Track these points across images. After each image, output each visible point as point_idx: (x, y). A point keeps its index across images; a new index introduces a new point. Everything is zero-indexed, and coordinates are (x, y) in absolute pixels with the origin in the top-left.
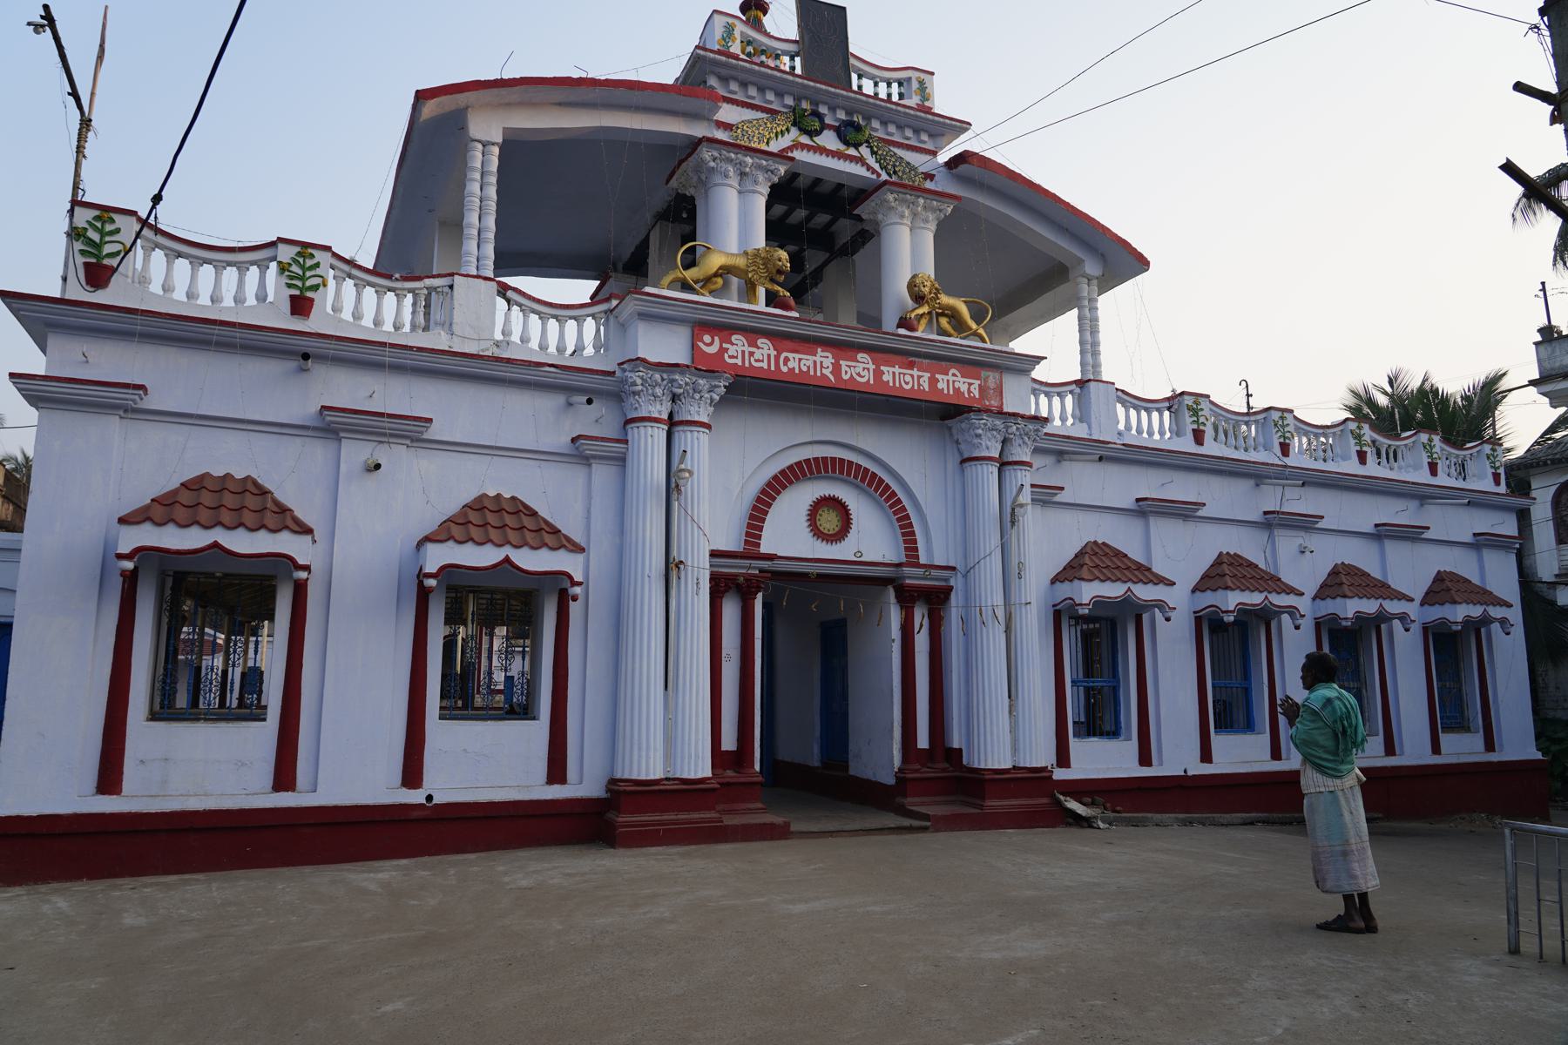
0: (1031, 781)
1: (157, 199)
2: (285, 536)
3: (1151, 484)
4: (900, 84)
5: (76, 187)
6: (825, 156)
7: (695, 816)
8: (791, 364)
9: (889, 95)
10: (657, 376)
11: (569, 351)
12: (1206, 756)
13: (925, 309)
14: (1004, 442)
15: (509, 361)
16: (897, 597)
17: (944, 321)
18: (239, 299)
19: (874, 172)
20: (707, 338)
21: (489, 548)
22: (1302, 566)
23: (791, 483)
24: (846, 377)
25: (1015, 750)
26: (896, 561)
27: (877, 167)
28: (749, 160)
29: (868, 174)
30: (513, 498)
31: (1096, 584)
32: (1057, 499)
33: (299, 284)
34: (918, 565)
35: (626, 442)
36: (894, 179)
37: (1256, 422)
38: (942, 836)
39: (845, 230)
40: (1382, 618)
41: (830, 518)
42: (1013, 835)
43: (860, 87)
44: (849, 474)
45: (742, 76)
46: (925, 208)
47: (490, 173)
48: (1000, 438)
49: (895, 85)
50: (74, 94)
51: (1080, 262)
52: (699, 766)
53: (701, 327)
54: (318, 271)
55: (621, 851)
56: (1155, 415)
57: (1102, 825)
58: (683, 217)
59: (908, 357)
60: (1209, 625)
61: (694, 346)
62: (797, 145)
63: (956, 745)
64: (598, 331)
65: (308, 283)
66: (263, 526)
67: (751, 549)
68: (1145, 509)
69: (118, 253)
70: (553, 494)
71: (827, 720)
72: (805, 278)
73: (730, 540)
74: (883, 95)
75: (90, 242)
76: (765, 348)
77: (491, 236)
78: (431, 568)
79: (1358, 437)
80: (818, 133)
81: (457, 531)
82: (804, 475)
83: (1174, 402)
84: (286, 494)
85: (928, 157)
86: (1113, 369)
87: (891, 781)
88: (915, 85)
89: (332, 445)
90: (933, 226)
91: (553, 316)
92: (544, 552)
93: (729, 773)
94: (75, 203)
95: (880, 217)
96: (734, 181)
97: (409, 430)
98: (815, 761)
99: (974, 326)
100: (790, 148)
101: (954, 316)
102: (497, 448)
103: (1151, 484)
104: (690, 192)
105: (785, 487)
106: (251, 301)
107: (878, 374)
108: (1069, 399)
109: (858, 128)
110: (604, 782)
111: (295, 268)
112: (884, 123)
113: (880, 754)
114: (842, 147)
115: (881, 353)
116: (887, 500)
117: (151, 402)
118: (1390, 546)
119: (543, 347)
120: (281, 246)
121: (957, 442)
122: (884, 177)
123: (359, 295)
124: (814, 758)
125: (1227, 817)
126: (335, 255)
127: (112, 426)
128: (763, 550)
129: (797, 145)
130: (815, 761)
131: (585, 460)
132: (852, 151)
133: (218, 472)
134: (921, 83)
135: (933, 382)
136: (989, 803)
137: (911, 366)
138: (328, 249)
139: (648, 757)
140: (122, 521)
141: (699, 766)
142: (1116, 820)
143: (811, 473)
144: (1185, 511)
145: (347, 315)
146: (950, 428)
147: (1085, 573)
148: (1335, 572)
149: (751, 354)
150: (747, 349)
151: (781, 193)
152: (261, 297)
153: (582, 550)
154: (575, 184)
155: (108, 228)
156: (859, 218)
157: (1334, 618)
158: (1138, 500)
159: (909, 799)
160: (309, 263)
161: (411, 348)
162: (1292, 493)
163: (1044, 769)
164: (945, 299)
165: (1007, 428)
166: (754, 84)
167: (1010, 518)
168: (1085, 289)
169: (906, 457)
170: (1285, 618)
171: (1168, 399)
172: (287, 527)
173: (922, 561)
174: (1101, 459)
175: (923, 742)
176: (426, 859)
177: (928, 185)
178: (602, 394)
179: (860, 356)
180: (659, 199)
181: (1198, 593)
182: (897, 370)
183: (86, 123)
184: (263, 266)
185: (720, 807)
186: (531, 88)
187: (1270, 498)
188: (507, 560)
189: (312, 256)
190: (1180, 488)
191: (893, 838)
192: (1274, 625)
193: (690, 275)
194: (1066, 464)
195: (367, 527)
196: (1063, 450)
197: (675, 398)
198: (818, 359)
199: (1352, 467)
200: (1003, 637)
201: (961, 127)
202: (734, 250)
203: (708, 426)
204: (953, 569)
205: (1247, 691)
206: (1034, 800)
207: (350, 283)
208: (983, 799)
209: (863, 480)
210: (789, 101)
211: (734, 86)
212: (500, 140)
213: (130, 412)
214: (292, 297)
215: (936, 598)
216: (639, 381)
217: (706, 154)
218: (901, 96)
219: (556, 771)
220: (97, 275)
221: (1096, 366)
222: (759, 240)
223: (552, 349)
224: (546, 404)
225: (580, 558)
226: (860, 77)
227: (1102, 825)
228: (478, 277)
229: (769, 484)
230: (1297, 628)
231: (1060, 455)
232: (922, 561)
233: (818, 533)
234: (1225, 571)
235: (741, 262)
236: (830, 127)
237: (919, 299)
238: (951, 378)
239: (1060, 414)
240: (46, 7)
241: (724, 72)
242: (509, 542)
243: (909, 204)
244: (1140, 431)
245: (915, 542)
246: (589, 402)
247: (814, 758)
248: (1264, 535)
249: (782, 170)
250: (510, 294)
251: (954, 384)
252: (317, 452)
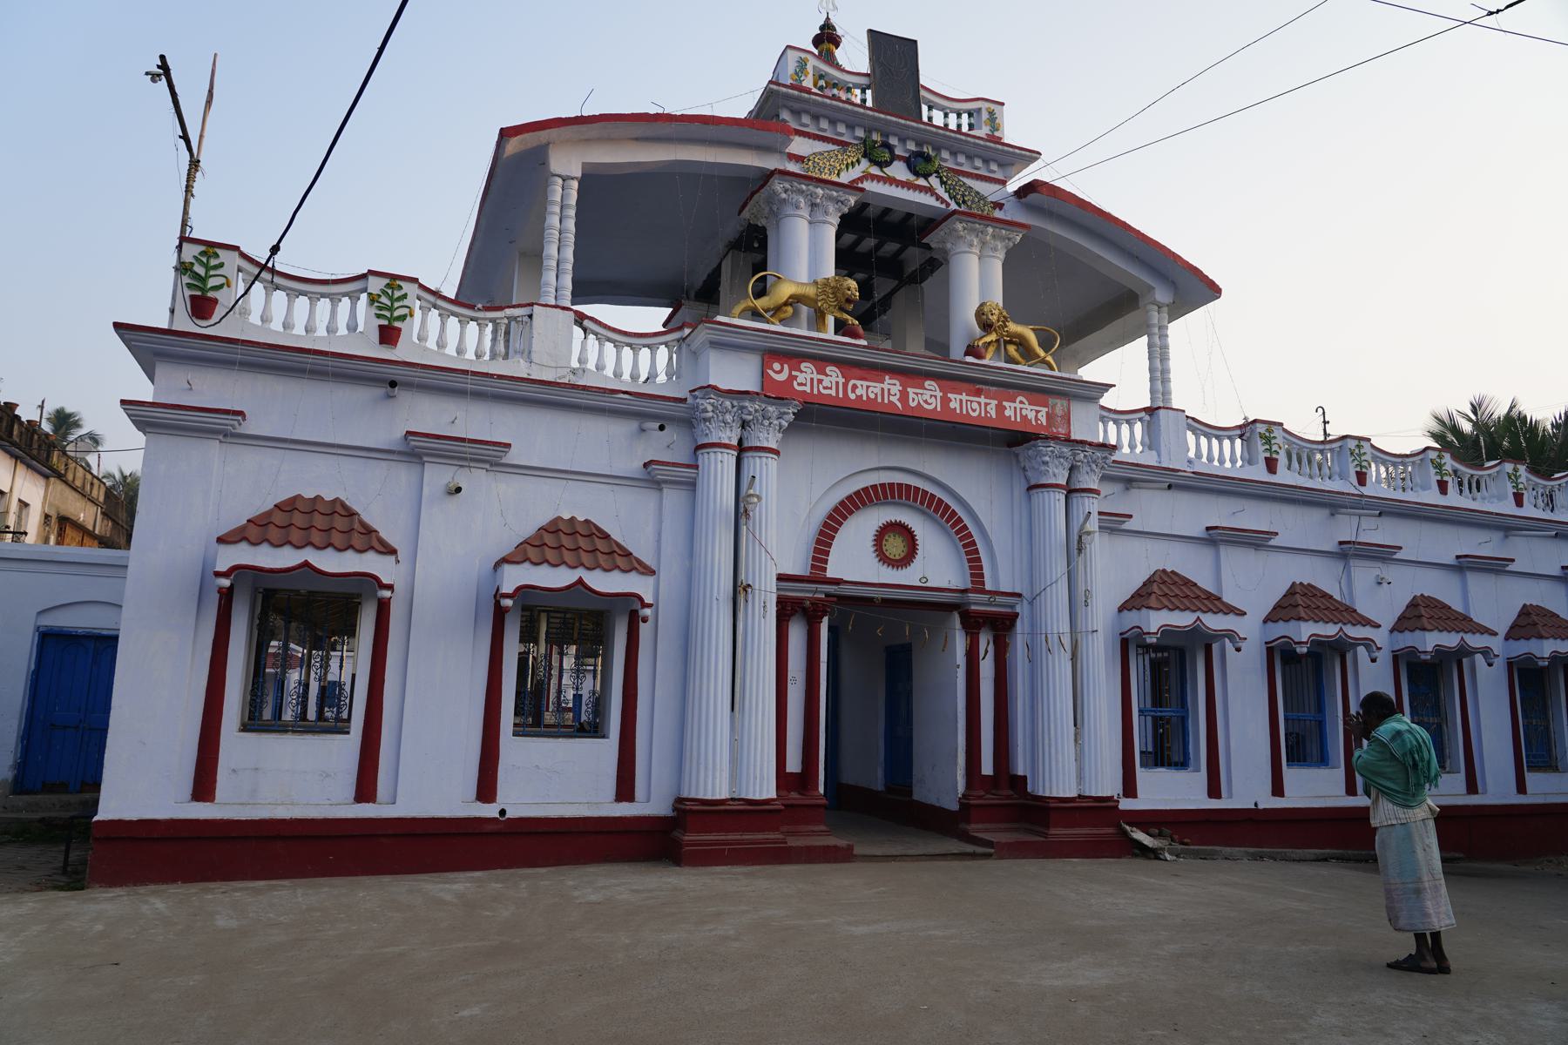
0: (1100, 809)
1: (275, 249)
2: (371, 556)
3: (1221, 513)
4: (970, 115)
5: (184, 224)
6: (896, 187)
7: (760, 836)
8: (859, 392)
9: (959, 126)
10: (728, 403)
11: (642, 379)
12: (1278, 790)
13: (993, 337)
14: (1072, 469)
15: (585, 388)
17: (1012, 349)
18: (331, 329)
19: (943, 201)
20: (777, 366)
21: (563, 569)
22: (1379, 598)
23: (858, 508)
24: (913, 404)
25: (1080, 778)
27: (946, 196)
28: (820, 191)
29: (937, 204)
30: (587, 521)
31: (1164, 612)
32: (1126, 526)
33: (388, 314)
34: (984, 592)
35: (696, 467)
36: (964, 208)
37: (1331, 450)
38: (1005, 863)
39: (914, 258)
40: (1463, 652)
41: (897, 544)
42: (1078, 865)
43: (930, 118)
44: (915, 500)
45: (814, 109)
46: (994, 236)
47: (569, 206)
48: (1067, 465)
49: (965, 116)
50: (185, 137)
51: (1151, 289)
52: (764, 787)
53: (771, 355)
54: (405, 302)
55: (687, 870)
56: (1226, 443)
57: (1169, 857)
58: (754, 248)
59: (974, 384)
60: (1280, 656)
61: (763, 374)
62: (867, 176)
63: (1020, 773)
64: (670, 358)
65: (396, 314)
66: (351, 547)
67: (817, 574)
68: (1215, 538)
69: (221, 287)
70: (626, 517)
71: (892, 745)
72: (873, 306)
73: (797, 564)
74: (953, 126)
75: (196, 276)
76: (833, 376)
77: (570, 267)
78: (508, 588)
79: (1439, 467)
80: (888, 164)
81: (532, 553)
82: (871, 501)
83: (1246, 431)
84: (372, 515)
85: (997, 187)
86: (1183, 397)
87: (955, 807)
88: (985, 116)
89: (417, 468)
90: (1001, 255)
91: (627, 343)
92: (616, 574)
93: (794, 795)
94: (184, 239)
95: (949, 246)
96: (805, 212)
97: (488, 455)
98: (880, 787)
99: (1042, 354)
100: (861, 179)
101: (1021, 343)
102: (572, 473)
103: (1221, 513)
104: (762, 222)
105: (851, 513)
106: (342, 331)
107: (945, 401)
108: (1138, 427)
109: (928, 159)
110: (671, 801)
111: (384, 299)
112: (954, 154)
113: (944, 779)
114: (911, 177)
115: (949, 381)
116: (953, 526)
117: (250, 427)
118: (1473, 579)
119: (618, 374)
120: (371, 278)
121: (1024, 469)
122: (954, 206)
123: (443, 324)
124: (876, 779)
125: (1299, 852)
126: (422, 287)
127: (213, 450)
128: (829, 574)
129: (867, 176)
130: (880, 787)
131: (657, 485)
132: (921, 182)
133: (309, 494)
134: (991, 113)
135: (1000, 409)
136: (1053, 831)
137: (978, 393)
138: (415, 280)
140: (220, 540)
141: (764, 787)
142: (1183, 851)
143: (878, 498)
144: (1257, 541)
145: (431, 344)
146: (1017, 456)
147: (1153, 601)
148: (1414, 604)
149: (820, 381)
150: (816, 376)
151: (848, 223)
152: (352, 327)
153: (653, 572)
154: (650, 215)
155: (213, 262)
156: (928, 247)
157: (1412, 652)
158: (1208, 529)
159: (973, 826)
160: (397, 294)
161: (492, 376)
162: (1367, 523)
163: (1110, 799)
164: (1013, 327)
165: (1074, 455)
166: (825, 117)
167: (1077, 546)
168: (1155, 317)
169: (972, 484)
170: (1361, 650)
171: (1240, 427)
172: (372, 548)
173: (988, 587)
174: (1170, 487)
175: (987, 768)
176: (499, 872)
177: (998, 214)
178: (672, 419)
179: (927, 383)
180: (732, 230)
181: (1270, 624)
182: (964, 397)
183: (194, 164)
184: (354, 297)
185: (784, 828)
186: (609, 125)
187: (1347, 528)
188: (580, 581)
189: (400, 288)
190: (1252, 517)
191: (955, 864)
192: (1349, 657)
193: (760, 303)
194: (1134, 492)
195: (447, 548)
196: (1131, 478)
197: (744, 425)
198: (886, 386)
199: (1432, 497)
200: (1069, 664)
201: (1031, 156)
202: (805, 280)
203: (777, 452)
204: (1019, 595)
205: (1321, 725)
206: (1099, 830)
207: (435, 312)
208: (1048, 827)
209: (929, 506)
210: (860, 133)
211: (806, 119)
212: (579, 174)
213: (228, 436)
214: (381, 327)
215: (1002, 625)
216: (710, 408)
217: (778, 186)
218: (971, 127)
219: (625, 790)
220: (202, 306)
221: (1166, 393)
222: (829, 269)
223: (626, 376)
224: (621, 429)
225: (651, 580)
226: (930, 108)
227: (1169, 857)
228: (556, 307)
229: (836, 509)
230: (1374, 660)
231: (1129, 483)
232: (988, 587)
233: (884, 558)
234: (1298, 601)
235: (811, 291)
236: (900, 158)
237: (987, 327)
238: (1018, 406)
239: (1128, 441)
240: (162, 57)
241: (797, 106)
242: (582, 565)
243: (977, 233)
244: (1210, 459)
245: (981, 568)
246: (662, 428)
247: (876, 779)
248: (1338, 566)
249: (852, 201)
250: (586, 323)
251: (1022, 411)
252: (402, 475)
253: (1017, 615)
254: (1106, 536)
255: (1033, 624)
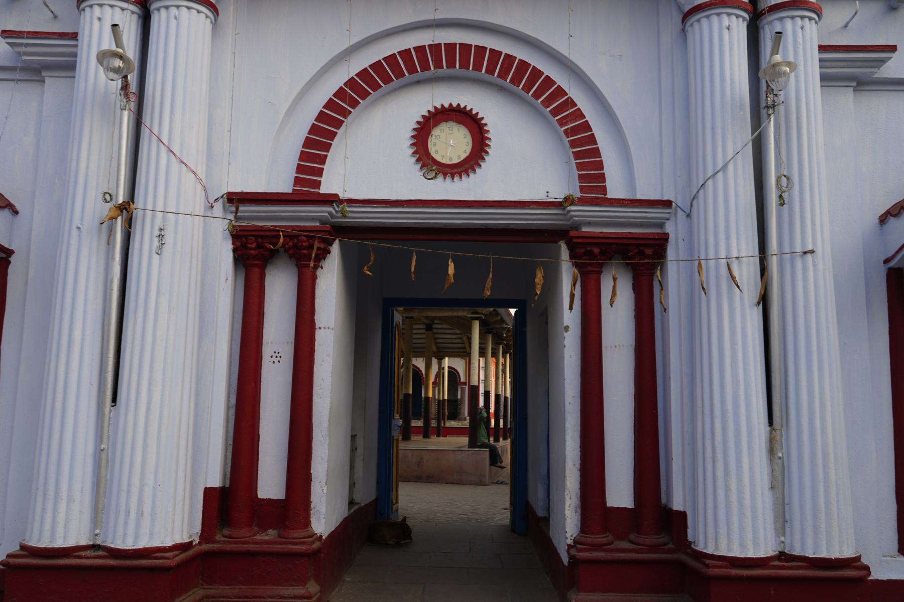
16: (572, 257)
25: (782, 520)
26: (558, 194)
35: (74, 36)
67: (306, 190)
128: (323, 190)
131: (33, 72)
139: (56, 512)
163: (853, 562)
167: (763, 98)
175: (620, 492)
204: (667, 204)
215: (642, 254)
253: (665, 238)
254: (846, 97)
255: (691, 249)
